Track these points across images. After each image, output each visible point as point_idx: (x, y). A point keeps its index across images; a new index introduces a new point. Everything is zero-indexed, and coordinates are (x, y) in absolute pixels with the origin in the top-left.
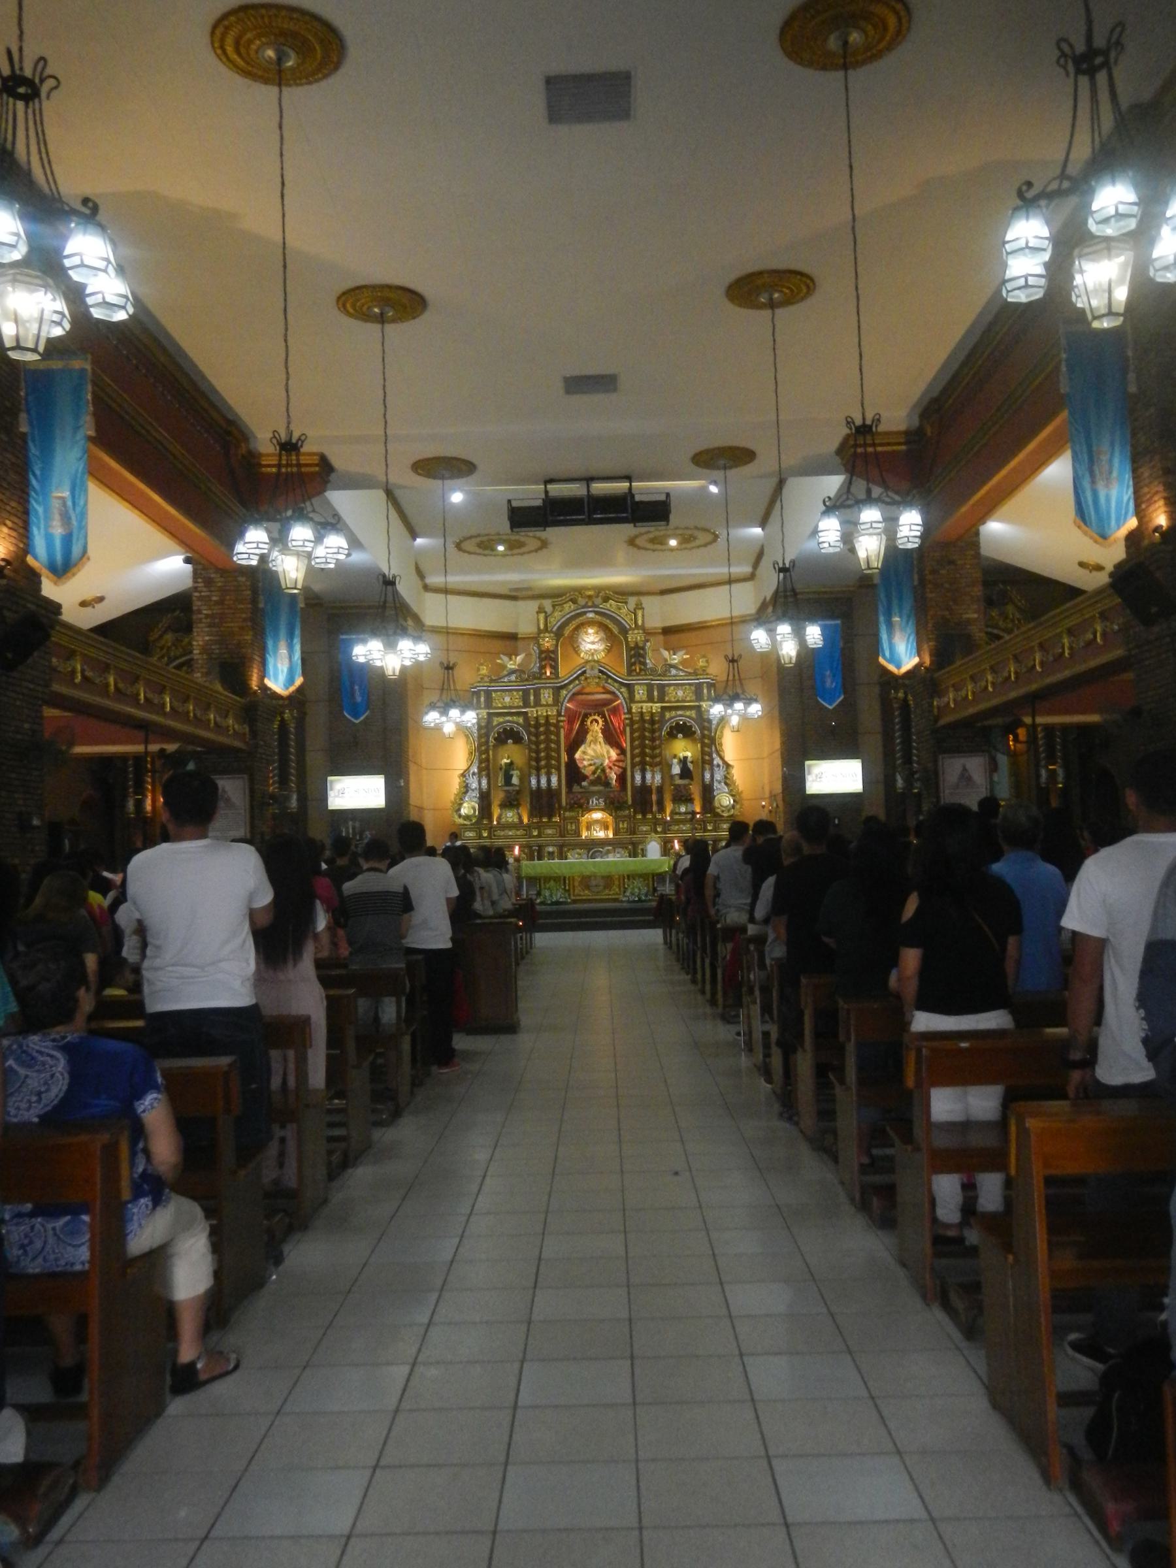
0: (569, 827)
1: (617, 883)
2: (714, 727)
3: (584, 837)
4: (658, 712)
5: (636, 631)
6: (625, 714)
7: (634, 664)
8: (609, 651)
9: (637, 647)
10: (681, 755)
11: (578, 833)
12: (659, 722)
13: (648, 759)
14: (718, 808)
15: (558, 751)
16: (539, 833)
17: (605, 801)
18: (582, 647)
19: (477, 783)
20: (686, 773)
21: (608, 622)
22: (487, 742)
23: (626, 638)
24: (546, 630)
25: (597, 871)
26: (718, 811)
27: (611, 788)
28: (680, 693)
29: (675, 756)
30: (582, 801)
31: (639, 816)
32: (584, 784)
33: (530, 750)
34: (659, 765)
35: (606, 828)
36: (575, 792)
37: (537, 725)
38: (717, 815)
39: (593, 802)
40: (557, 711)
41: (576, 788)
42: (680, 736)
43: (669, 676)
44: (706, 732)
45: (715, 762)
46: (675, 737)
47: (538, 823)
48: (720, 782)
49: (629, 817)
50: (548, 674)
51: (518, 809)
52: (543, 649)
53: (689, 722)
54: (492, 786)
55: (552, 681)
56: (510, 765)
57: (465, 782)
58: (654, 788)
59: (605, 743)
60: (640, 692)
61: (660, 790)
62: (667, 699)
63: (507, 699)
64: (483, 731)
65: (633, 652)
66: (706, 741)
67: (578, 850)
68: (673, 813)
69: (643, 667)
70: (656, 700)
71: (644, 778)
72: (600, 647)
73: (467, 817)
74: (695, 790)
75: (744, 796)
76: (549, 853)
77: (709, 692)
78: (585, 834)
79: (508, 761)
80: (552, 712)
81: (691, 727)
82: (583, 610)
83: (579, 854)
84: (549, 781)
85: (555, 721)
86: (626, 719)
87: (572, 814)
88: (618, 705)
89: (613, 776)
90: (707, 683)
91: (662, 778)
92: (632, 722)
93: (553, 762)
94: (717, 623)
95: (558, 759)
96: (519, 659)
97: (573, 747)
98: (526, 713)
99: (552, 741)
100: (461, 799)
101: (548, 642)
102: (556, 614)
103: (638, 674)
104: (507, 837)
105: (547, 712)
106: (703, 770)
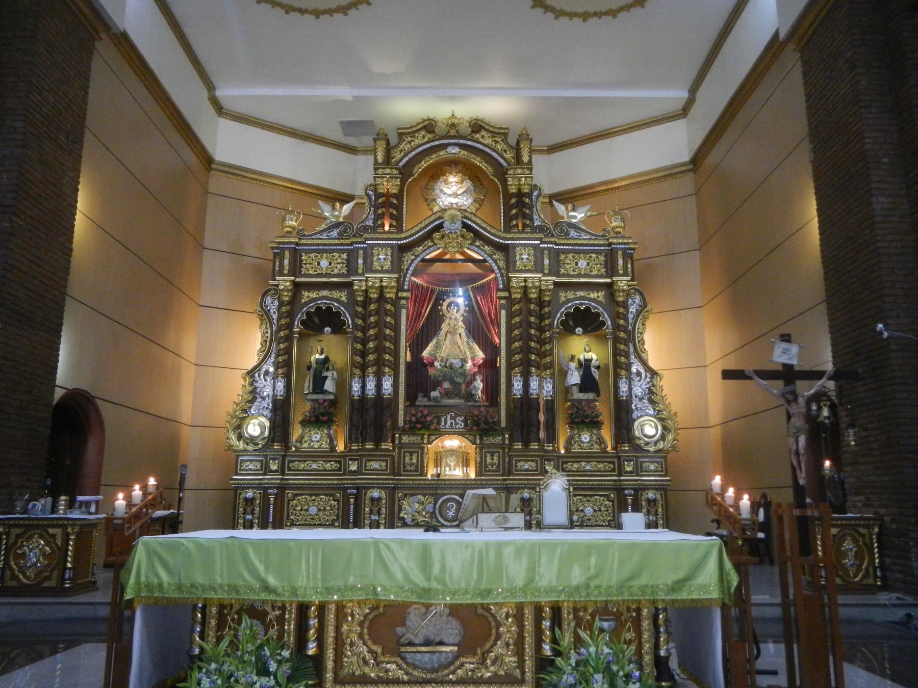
0: (407, 459)
1: (509, 629)
2: (631, 316)
3: (429, 477)
4: (549, 290)
5: (519, 171)
6: (498, 290)
7: (516, 217)
8: (479, 202)
9: (520, 194)
10: (582, 358)
11: (420, 469)
12: (549, 303)
13: (533, 357)
14: (639, 439)
15: (396, 341)
16: (360, 467)
17: (465, 421)
18: (438, 200)
19: (271, 389)
20: (588, 383)
21: (478, 161)
22: (290, 326)
23: (504, 182)
24: (387, 161)
25: (434, 585)
26: (638, 442)
27: (476, 401)
28: (582, 263)
29: (572, 358)
30: (429, 419)
31: (518, 446)
32: (434, 394)
33: (355, 340)
34: (550, 368)
35: (466, 463)
36: (420, 406)
37: (367, 301)
38: (638, 449)
39: (446, 423)
40: (398, 280)
41: (421, 401)
42: (579, 330)
43: (570, 239)
44: (622, 322)
45: (634, 370)
46: (574, 333)
47: (357, 451)
48: (641, 399)
49: (502, 446)
50: (387, 228)
51: (329, 428)
52: (381, 191)
53: (594, 307)
54: (293, 394)
55: (391, 236)
56: (325, 363)
57: (252, 384)
58: (542, 403)
59: (468, 337)
60: (524, 257)
61: (550, 406)
62: (562, 271)
63: (324, 263)
64: (284, 309)
65: (513, 201)
66: (622, 335)
67: (420, 497)
68: (569, 443)
69: (528, 222)
70: (546, 271)
71: (526, 385)
72: (466, 202)
73: (252, 440)
74: (604, 409)
75: (681, 421)
76: (373, 500)
77: (625, 264)
78: (431, 472)
79: (322, 357)
80: (389, 280)
81: (598, 315)
82: (442, 142)
83: (422, 503)
84: (379, 386)
85: (392, 296)
86: (500, 298)
87: (413, 439)
88: (489, 283)
89: (479, 384)
90: (624, 250)
91: (553, 388)
92: (511, 301)
93: (387, 357)
94: (629, 182)
95: (396, 354)
96: (347, 208)
97: (419, 341)
98: (351, 284)
99: (386, 325)
100: (245, 411)
101: (388, 181)
102: (405, 146)
103: (523, 232)
104: (305, 472)
105: (381, 281)
106: (617, 377)
